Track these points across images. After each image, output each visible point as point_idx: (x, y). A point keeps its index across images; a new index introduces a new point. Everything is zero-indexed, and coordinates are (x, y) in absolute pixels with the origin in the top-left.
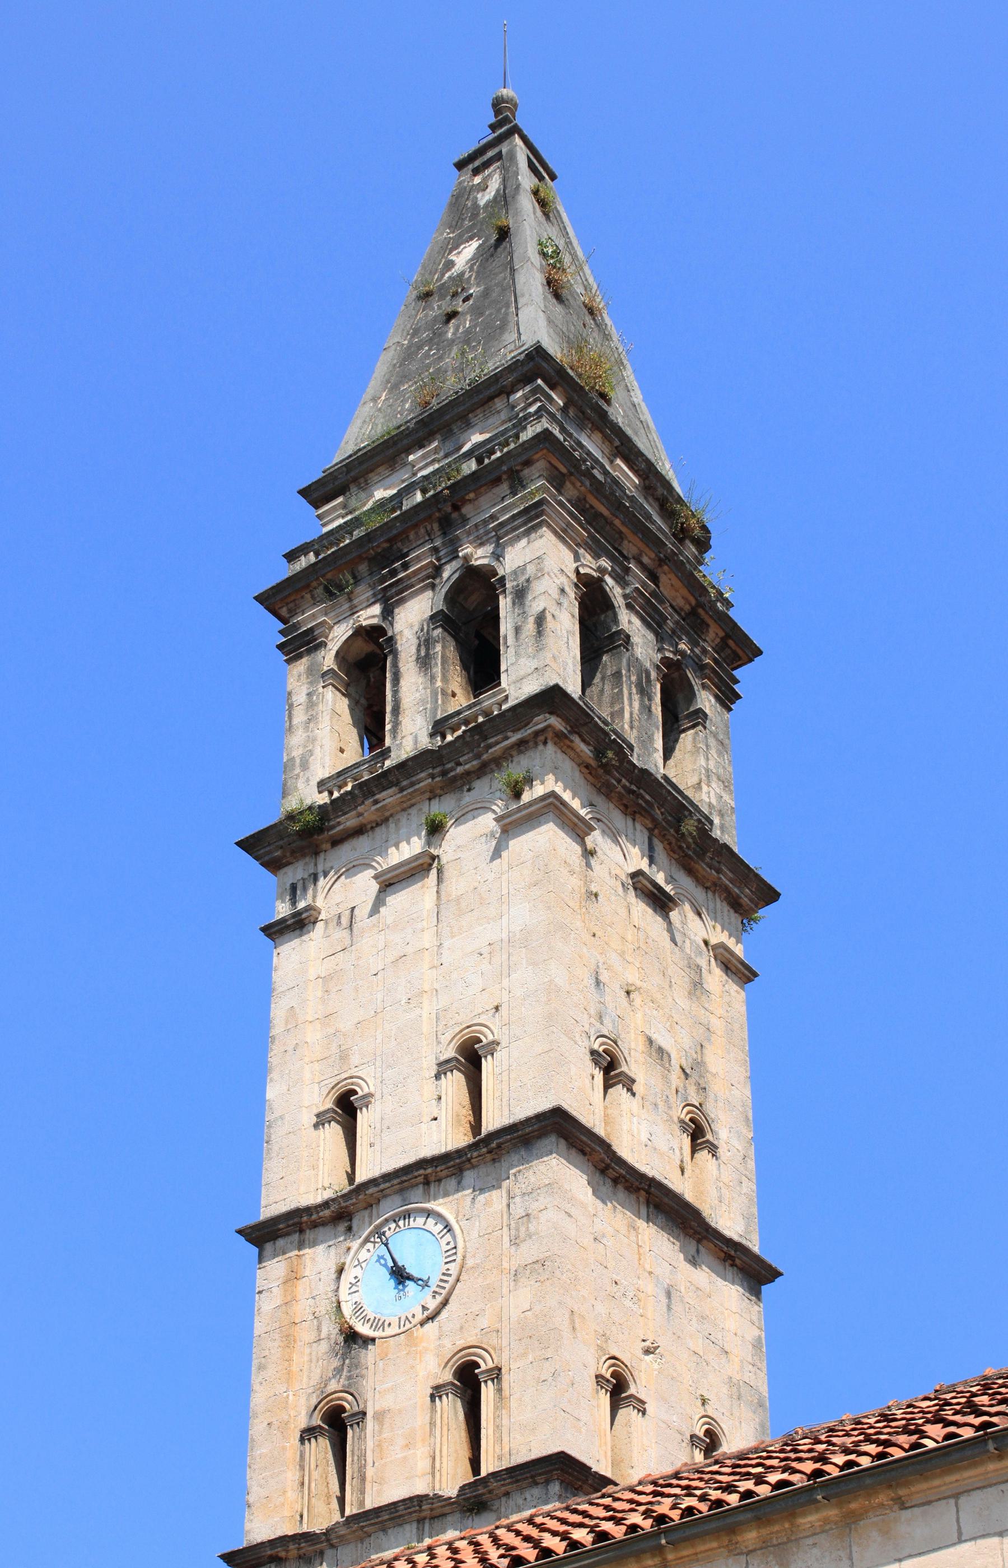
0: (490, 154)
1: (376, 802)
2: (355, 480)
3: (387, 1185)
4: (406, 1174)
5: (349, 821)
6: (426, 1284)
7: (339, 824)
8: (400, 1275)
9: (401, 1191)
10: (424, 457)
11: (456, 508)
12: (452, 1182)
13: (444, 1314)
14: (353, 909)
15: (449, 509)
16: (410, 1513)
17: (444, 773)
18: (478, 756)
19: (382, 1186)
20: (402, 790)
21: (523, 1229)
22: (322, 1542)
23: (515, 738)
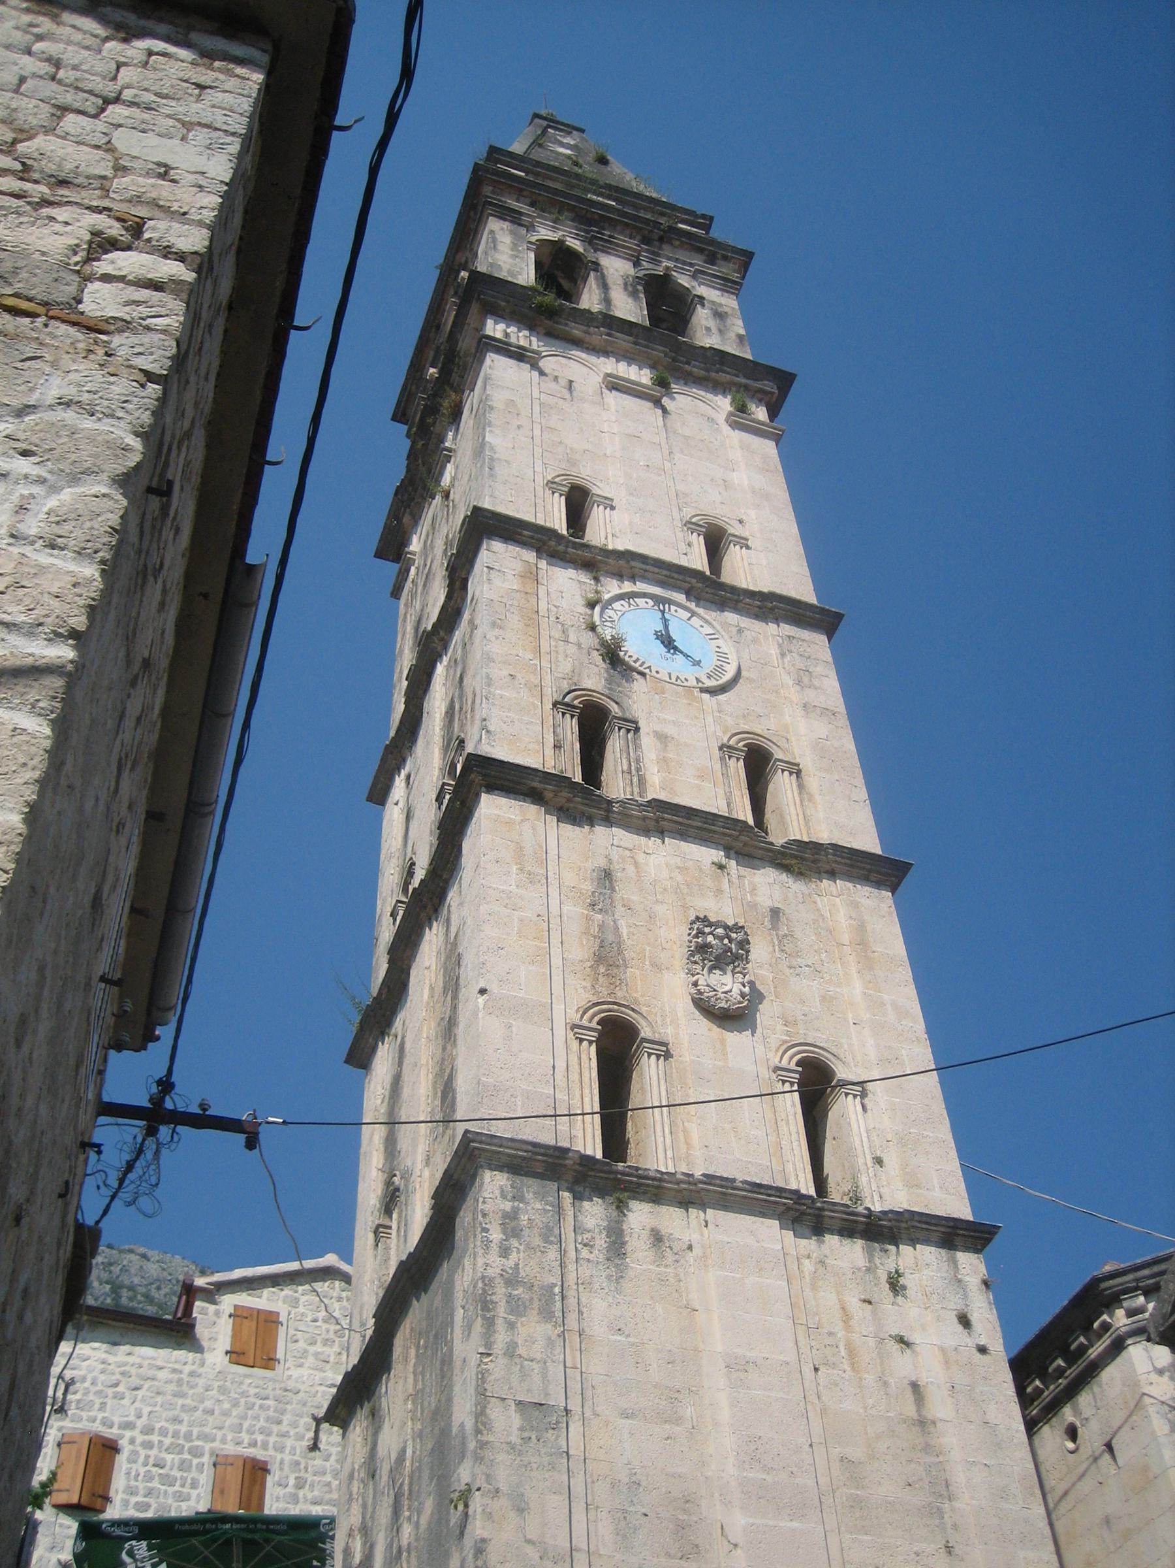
1: (609, 335)
3: (656, 570)
4: (679, 573)
5: (577, 331)
7: (566, 325)
8: (668, 643)
11: (661, 239)
13: (722, 697)
14: (571, 382)
15: (656, 237)
16: (725, 834)
17: (674, 360)
18: (708, 371)
19: (648, 567)
20: (635, 343)
21: (806, 680)
22: (599, 809)
23: (743, 381)
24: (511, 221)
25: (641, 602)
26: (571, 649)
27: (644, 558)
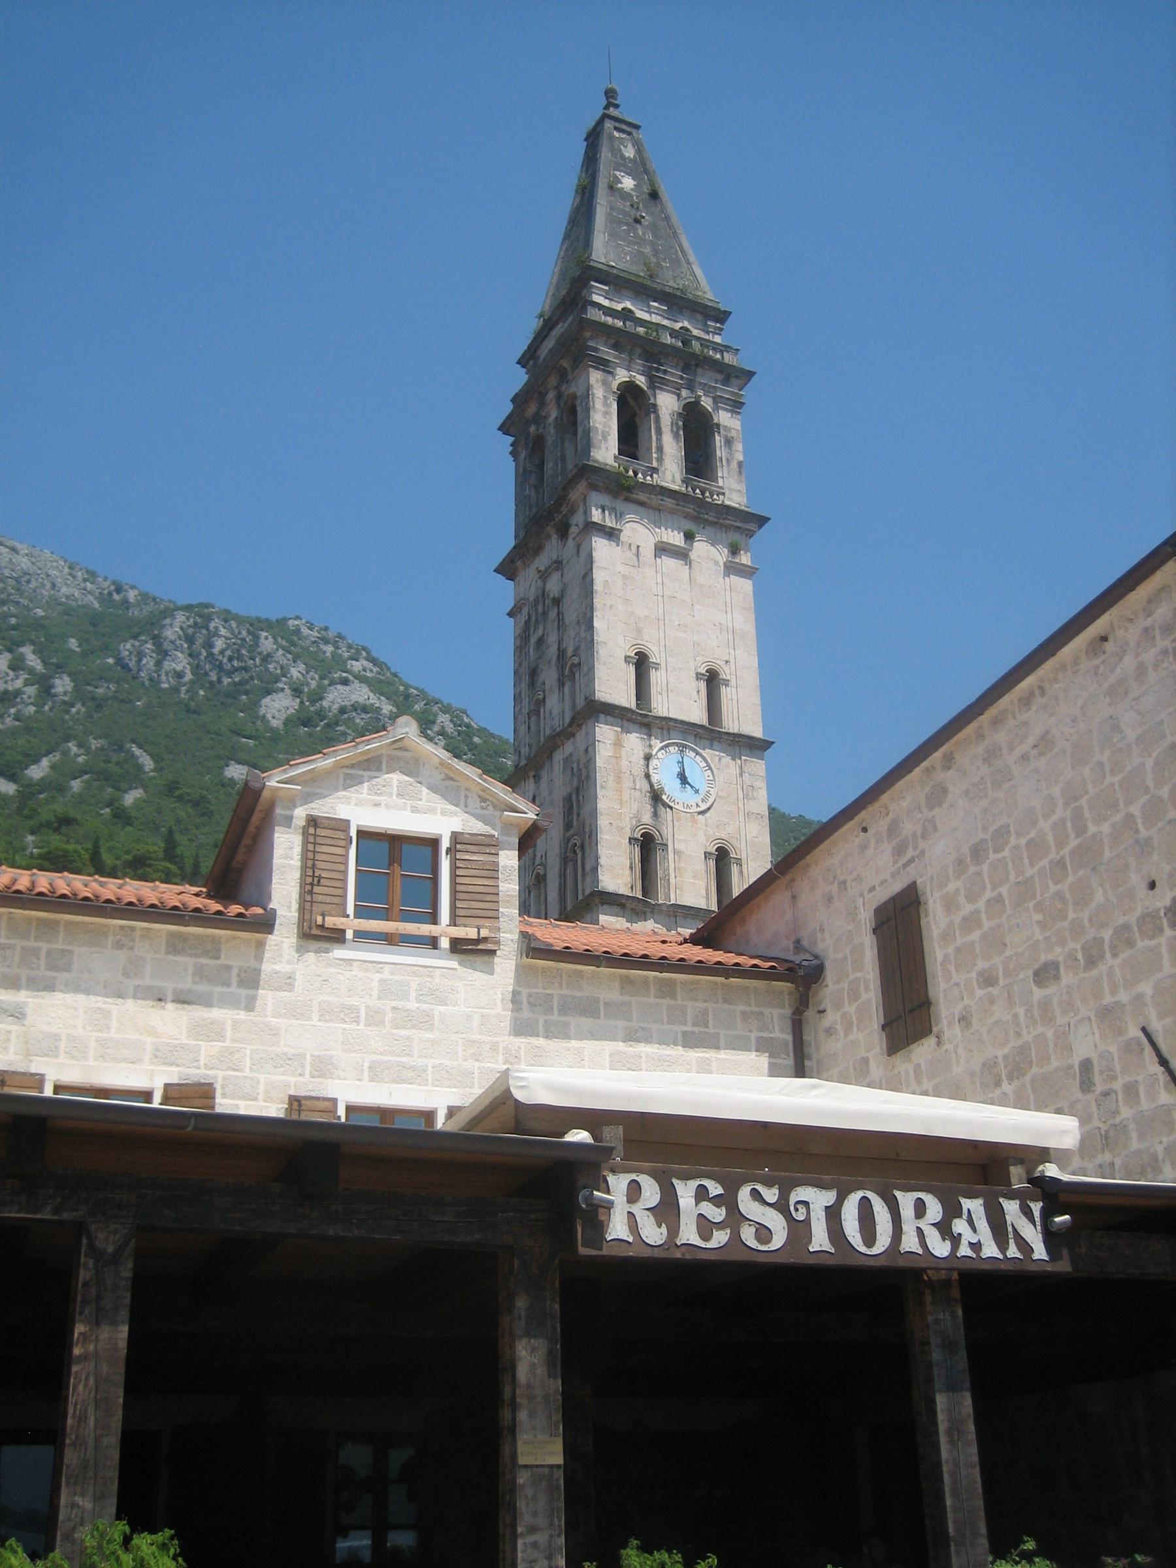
0: (624, 127)
2: (616, 285)
5: (642, 497)
6: (697, 791)
8: (683, 779)
9: (683, 732)
10: (657, 308)
11: (697, 365)
12: (707, 743)
13: (708, 815)
17: (699, 513)
24: (603, 371)
25: (671, 748)
26: (638, 793)
27: (675, 720)
